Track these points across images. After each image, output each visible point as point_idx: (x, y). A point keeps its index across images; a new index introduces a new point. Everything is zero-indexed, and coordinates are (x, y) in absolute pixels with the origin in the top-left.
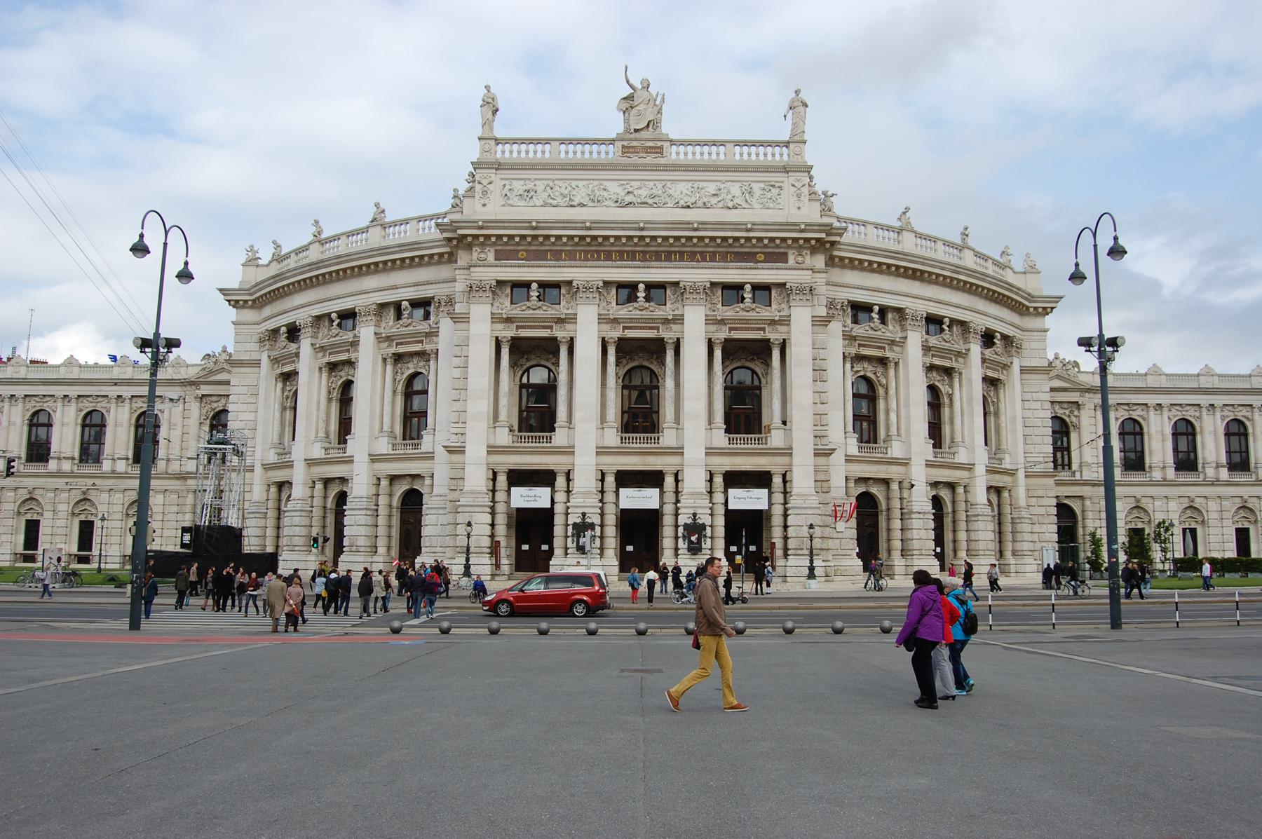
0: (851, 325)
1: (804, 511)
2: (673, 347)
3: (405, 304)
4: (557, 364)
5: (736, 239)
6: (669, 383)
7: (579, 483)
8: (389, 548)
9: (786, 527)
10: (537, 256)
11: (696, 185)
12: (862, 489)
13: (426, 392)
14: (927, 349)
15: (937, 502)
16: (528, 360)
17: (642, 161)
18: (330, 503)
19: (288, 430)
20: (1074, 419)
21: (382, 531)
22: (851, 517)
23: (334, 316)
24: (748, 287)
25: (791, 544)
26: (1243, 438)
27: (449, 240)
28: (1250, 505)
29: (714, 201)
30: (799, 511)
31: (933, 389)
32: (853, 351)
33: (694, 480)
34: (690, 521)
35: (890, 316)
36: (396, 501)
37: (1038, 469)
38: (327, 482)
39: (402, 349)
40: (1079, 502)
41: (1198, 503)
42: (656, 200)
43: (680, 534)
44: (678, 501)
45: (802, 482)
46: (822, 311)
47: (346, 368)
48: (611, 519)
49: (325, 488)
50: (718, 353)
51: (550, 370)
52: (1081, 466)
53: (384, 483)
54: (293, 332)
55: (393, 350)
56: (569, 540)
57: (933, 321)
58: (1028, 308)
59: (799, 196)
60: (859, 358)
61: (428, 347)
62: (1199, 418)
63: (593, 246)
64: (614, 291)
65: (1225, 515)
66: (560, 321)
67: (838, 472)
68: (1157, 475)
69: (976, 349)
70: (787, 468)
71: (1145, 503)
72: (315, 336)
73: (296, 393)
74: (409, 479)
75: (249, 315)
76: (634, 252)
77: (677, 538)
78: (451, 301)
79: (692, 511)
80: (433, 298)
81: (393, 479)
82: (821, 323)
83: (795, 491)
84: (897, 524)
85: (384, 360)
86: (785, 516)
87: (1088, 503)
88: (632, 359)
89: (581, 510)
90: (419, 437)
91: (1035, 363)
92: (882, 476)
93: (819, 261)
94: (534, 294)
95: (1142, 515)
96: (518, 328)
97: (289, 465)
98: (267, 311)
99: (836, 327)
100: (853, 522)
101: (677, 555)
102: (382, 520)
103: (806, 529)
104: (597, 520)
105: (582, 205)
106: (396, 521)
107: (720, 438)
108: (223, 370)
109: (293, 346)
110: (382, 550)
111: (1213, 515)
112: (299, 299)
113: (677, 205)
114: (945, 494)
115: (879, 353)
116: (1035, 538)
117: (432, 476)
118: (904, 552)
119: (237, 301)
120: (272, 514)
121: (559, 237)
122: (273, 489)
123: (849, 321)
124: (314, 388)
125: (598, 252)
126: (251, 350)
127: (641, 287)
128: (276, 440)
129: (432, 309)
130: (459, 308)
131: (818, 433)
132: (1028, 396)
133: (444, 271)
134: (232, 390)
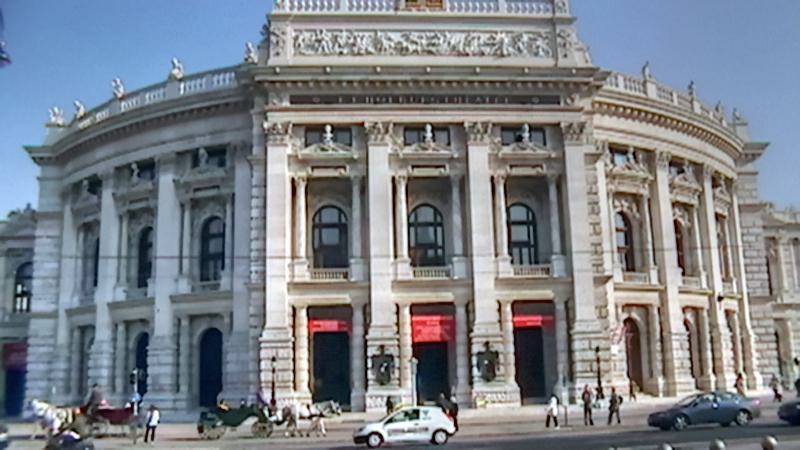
0: (611, 166)
2: (458, 183)
3: (202, 151)
4: (350, 204)
5: (514, 83)
6: (457, 219)
7: (377, 318)
8: (190, 386)
9: (570, 352)
10: (329, 101)
11: (473, 35)
12: (625, 316)
13: (223, 235)
14: (672, 186)
15: (686, 323)
16: (320, 201)
17: (421, 14)
18: (132, 344)
19: (90, 280)
21: (183, 369)
22: (620, 339)
23: (134, 166)
24: (527, 127)
25: (579, 367)
27: (246, 86)
29: (487, 50)
31: (676, 222)
32: (612, 187)
34: (483, 349)
35: (640, 156)
36: (196, 340)
37: (759, 293)
38: (128, 324)
39: (200, 194)
42: (440, 48)
44: (470, 330)
45: (584, 311)
46: (592, 149)
47: (145, 215)
48: (408, 350)
49: (127, 329)
50: (500, 189)
51: (340, 210)
53: (185, 323)
54: (95, 185)
55: (191, 195)
56: (369, 372)
57: (676, 164)
59: (565, 45)
60: (618, 195)
61: (224, 191)
63: (378, 90)
64: (401, 132)
66: (352, 161)
67: (613, 297)
69: (708, 185)
72: (116, 186)
73: (98, 241)
74: (208, 319)
75: (52, 171)
76: (420, 96)
77: (471, 367)
78: (247, 147)
79: (485, 340)
80: (229, 144)
81: (193, 318)
82: (593, 158)
83: (578, 317)
85: (182, 206)
86: (570, 340)
88: (417, 198)
89: (379, 343)
90: (216, 277)
91: (749, 201)
93: (585, 103)
94: (329, 135)
96: (313, 168)
97: (92, 309)
98: (69, 167)
99: (600, 165)
100: (622, 344)
102: (183, 360)
103: (593, 352)
104: (394, 351)
105: (369, 53)
106: (196, 360)
107: (507, 270)
108: (26, 227)
109: (94, 199)
110: (184, 388)
112: (100, 153)
113: (460, 54)
115: (633, 190)
117: (231, 315)
118: (664, 373)
119: (41, 158)
120: (76, 358)
121: (350, 82)
122: (77, 334)
123: (608, 162)
124: (113, 236)
125: (387, 97)
126: (52, 204)
127: (429, 128)
128: (79, 286)
129: (228, 157)
130: (256, 150)
131: (594, 262)
132: (745, 231)
133: (238, 120)
134: (38, 241)
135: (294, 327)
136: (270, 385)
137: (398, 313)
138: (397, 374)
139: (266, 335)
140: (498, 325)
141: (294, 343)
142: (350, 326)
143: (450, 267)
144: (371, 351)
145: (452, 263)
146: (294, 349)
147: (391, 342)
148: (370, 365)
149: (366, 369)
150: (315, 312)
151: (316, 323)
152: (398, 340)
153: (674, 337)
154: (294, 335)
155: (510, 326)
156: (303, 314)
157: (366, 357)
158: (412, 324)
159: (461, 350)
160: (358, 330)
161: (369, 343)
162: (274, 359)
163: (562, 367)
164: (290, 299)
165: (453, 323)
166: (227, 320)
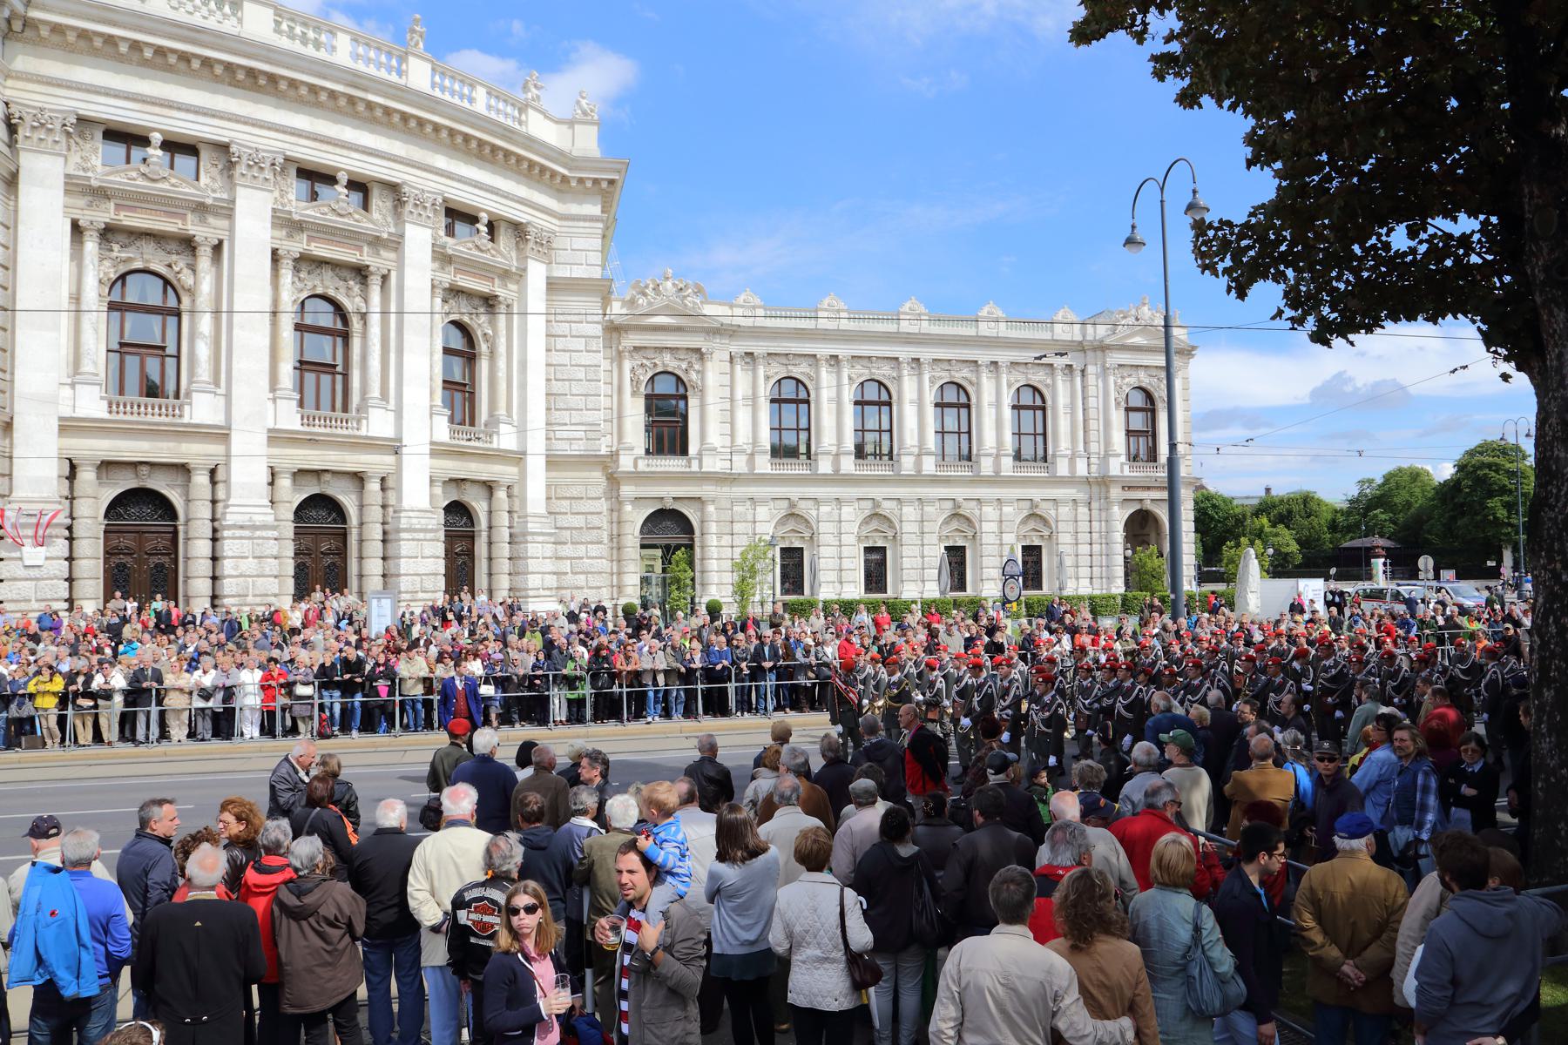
12: (127, 483)
20: (694, 376)
26: (964, 412)
28: (967, 513)
37: (578, 448)
40: (697, 505)
41: (888, 508)
52: (700, 454)
58: (565, 179)
62: (899, 379)
65: (928, 527)
68: (825, 466)
69: (420, 238)
71: (804, 508)
84: (202, 548)
87: (711, 508)
95: (801, 528)
111: (909, 528)
116: (566, 566)
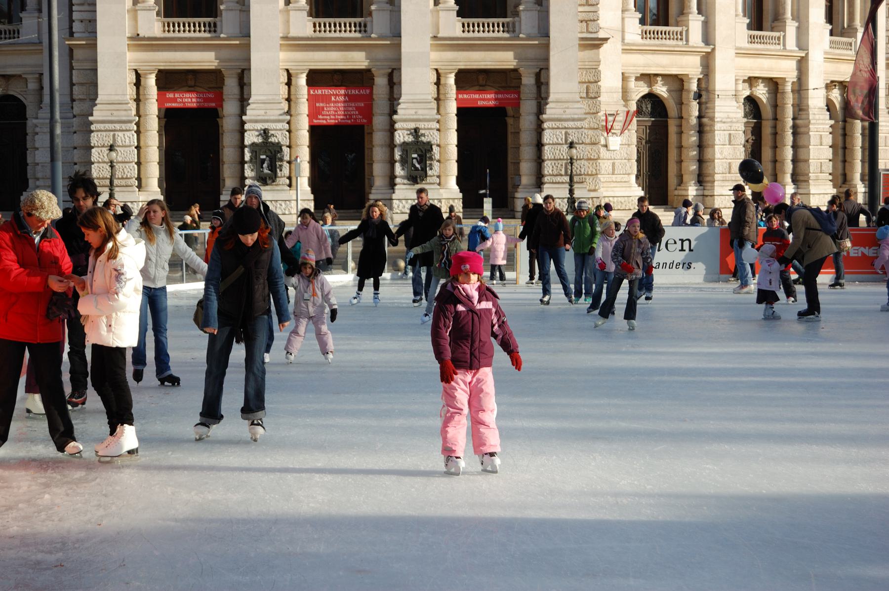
1: (566, 124)
9: (539, 145)
12: (645, 90)
30: (558, 124)
33: (416, 84)
43: (397, 156)
45: (563, 85)
70: (541, 64)
77: (392, 162)
79: (412, 125)
86: (539, 130)
89: (260, 126)
92: (674, 71)
100: (632, 135)
101: (392, 185)
114: (762, 92)
135: (138, 100)
136: (108, 182)
137: (289, 84)
138: (286, 171)
139: (98, 114)
140: (434, 105)
141: (138, 124)
142: (220, 99)
143: (368, 19)
144: (251, 138)
145: (370, 14)
146: (138, 132)
147: (279, 126)
148: (247, 156)
149: (242, 162)
150: (168, 80)
151: (170, 95)
152: (289, 123)
153: (717, 126)
154: (138, 114)
155: (452, 108)
156: (151, 81)
157: (242, 146)
158: (312, 99)
159: (379, 137)
160: (230, 108)
161: (246, 127)
162: (111, 148)
163: (526, 167)
164: (133, 58)
165: (370, 98)
166: (32, 86)
